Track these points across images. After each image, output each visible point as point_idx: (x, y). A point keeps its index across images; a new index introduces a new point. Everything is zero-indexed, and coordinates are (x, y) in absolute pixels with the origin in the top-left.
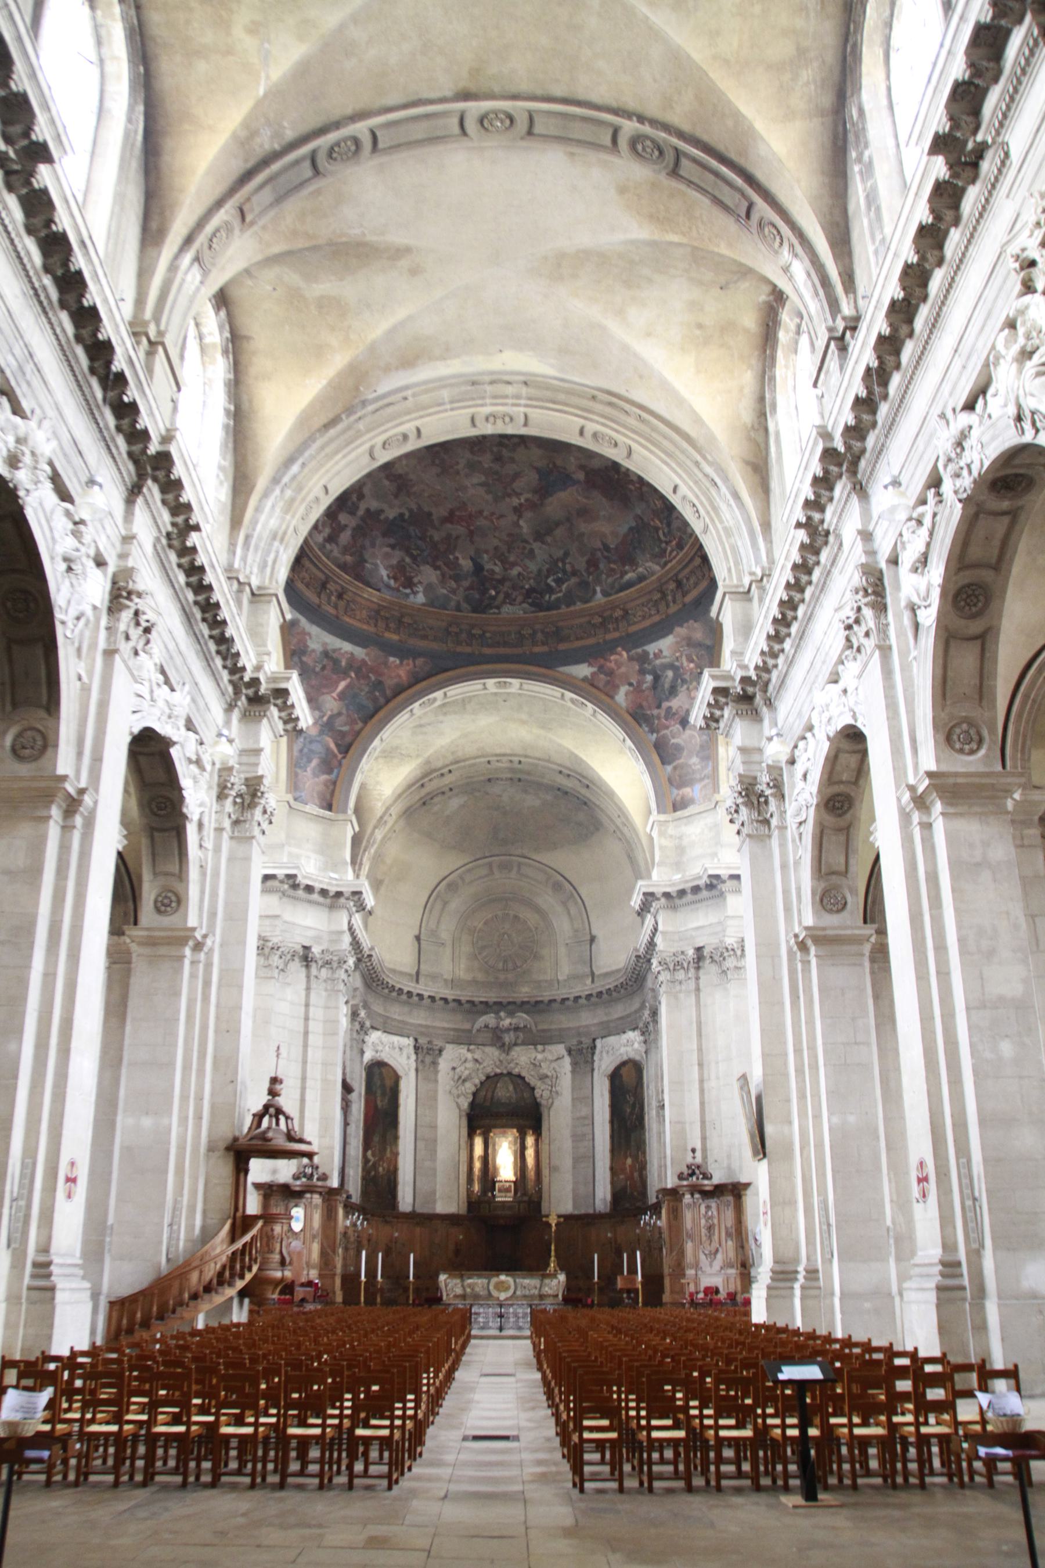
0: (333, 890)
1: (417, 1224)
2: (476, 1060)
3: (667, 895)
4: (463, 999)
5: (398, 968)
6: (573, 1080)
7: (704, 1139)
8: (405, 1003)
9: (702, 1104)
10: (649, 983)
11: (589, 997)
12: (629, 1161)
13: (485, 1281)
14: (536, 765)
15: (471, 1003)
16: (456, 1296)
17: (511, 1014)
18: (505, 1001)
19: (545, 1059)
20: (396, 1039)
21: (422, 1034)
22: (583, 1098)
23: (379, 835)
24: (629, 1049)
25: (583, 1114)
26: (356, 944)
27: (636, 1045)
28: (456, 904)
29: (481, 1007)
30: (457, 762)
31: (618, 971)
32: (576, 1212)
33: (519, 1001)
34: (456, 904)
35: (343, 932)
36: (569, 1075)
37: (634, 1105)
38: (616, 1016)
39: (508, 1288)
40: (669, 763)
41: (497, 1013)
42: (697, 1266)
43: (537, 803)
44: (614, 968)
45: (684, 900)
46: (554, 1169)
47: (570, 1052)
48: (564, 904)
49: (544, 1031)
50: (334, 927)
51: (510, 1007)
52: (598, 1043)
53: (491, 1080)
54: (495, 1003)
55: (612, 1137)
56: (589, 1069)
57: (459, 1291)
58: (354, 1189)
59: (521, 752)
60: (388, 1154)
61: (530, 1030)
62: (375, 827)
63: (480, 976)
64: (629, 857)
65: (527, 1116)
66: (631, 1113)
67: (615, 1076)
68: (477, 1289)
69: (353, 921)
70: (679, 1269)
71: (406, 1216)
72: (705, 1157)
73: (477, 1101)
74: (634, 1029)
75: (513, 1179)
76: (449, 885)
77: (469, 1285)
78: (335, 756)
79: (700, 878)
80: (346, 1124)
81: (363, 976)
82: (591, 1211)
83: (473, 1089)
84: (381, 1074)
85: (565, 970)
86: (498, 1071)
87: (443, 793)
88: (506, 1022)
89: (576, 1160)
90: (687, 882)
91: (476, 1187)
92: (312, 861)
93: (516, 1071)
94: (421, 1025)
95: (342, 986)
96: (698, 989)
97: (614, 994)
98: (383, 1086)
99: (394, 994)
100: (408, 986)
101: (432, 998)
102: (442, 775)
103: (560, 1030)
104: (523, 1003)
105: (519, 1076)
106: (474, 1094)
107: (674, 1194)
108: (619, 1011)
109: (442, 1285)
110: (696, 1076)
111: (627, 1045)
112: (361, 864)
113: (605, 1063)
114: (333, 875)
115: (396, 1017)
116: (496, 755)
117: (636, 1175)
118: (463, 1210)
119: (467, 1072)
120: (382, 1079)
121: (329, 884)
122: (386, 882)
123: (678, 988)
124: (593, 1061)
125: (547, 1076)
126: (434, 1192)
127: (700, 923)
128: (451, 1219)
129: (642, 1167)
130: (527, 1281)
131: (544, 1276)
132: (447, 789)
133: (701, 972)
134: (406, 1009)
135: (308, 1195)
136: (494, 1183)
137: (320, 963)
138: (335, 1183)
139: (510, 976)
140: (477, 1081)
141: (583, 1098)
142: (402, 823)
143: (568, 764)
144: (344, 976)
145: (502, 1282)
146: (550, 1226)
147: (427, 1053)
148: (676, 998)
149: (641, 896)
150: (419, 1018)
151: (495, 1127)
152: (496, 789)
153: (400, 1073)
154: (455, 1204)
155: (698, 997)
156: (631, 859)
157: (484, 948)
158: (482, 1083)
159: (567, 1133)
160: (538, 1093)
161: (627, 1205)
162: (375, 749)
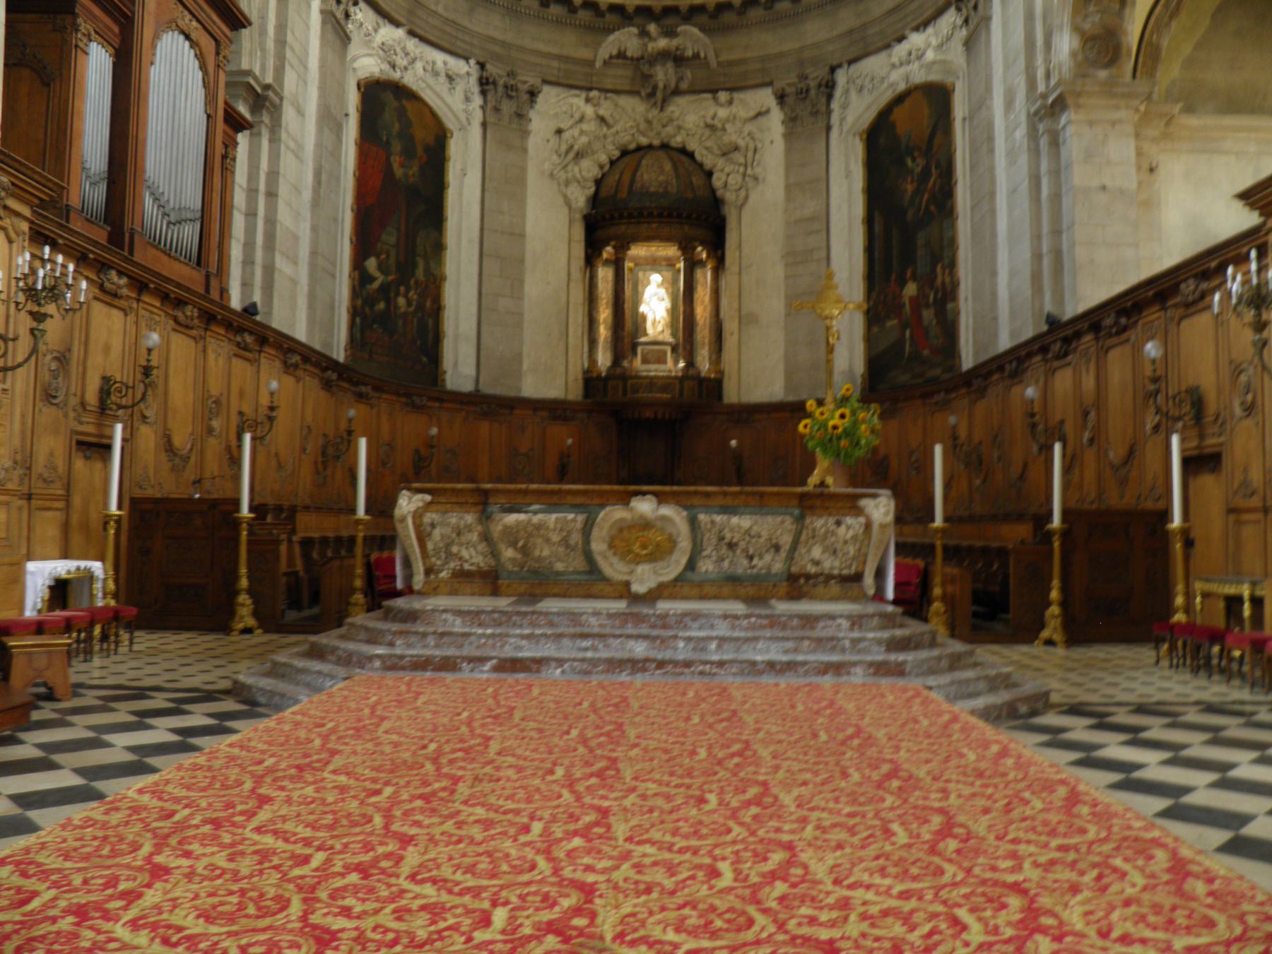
2: (602, 119)
6: (788, 151)
12: (911, 289)
13: (574, 519)
17: (670, 33)
19: (732, 119)
20: (440, 58)
21: (497, 57)
22: (808, 182)
27: (930, 55)
29: (610, 18)
37: (926, 173)
38: (885, 8)
39: (657, 554)
46: (746, 320)
47: (781, 98)
49: (730, 63)
52: (841, 77)
55: (869, 250)
57: (473, 556)
60: (420, 272)
61: (706, 64)
65: (699, 223)
66: (918, 191)
73: (603, 194)
77: (511, 536)
83: (595, 172)
84: (402, 113)
86: (644, 141)
88: (663, 43)
91: (604, 359)
93: (677, 141)
94: (493, 40)
106: (598, 182)
109: (408, 532)
113: (855, 108)
115: (440, 10)
117: (928, 315)
118: (575, 393)
119: (584, 139)
124: (829, 112)
125: (737, 148)
126: (518, 358)
128: (554, 410)
130: (742, 522)
136: (634, 346)
140: (604, 158)
141: (808, 182)
145: (645, 524)
147: (505, 95)
153: (450, 123)
154: (560, 382)
158: (612, 163)
160: (717, 181)
161: (904, 378)
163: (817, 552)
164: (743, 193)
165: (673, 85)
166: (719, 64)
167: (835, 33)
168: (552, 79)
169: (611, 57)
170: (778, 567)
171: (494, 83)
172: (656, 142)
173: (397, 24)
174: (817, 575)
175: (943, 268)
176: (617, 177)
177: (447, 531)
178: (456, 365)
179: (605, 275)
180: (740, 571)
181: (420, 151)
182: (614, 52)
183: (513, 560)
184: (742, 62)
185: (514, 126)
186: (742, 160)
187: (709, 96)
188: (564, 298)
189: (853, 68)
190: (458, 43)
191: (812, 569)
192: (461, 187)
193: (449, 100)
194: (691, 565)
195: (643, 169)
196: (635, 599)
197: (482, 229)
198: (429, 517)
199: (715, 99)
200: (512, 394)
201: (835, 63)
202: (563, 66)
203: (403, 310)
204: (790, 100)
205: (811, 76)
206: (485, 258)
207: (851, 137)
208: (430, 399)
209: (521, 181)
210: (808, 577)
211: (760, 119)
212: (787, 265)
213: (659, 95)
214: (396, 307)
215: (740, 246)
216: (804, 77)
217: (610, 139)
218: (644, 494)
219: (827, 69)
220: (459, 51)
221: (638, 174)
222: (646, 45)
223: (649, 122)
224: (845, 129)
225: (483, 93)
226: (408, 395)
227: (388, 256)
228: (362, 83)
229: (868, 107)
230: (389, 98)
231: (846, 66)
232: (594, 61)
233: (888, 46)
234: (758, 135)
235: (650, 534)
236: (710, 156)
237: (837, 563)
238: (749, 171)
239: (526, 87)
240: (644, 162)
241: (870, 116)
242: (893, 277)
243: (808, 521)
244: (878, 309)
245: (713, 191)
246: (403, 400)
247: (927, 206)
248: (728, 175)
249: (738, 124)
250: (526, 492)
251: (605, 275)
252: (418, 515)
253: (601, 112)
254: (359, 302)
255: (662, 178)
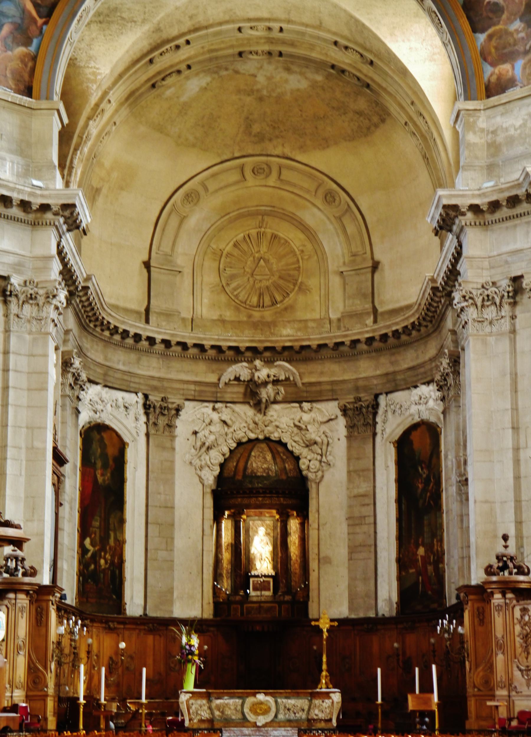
0: (36, 202)
1: (150, 631)
2: (224, 422)
3: (475, 209)
4: (207, 344)
5: (121, 304)
6: (349, 448)
7: (519, 523)
8: (132, 349)
9: (517, 478)
10: (449, 323)
11: (370, 341)
12: (421, 551)
13: (239, 701)
14: (303, 34)
15: (218, 349)
16: (201, 721)
17: (269, 362)
18: (260, 346)
20: (119, 395)
21: (155, 389)
23: (94, 129)
24: (422, 408)
25: (362, 491)
26: (67, 274)
27: (431, 403)
28: (198, 218)
30: (196, 30)
31: (408, 307)
32: (353, 616)
33: (278, 346)
34: (198, 218)
35: (52, 257)
36: (344, 442)
37: (427, 481)
38: (406, 366)
39: (266, 712)
40: (482, 31)
41: (250, 361)
42: (510, 685)
43: (304, 84)
44: (403, 303)
45: (498, 215)
46: (323, 561)
47: (344, 411)
48: (339, 219)
49: (311, 384)
50: (39, 251)
51: (267, 354)
52: (382, 400)
53: (244, 447)
54: (248, 349)
55: (399, 520)
56: (369, 433)
57: (205, 714)
58: (69, 586)
59: (283, 16)
60: (112, 542)
61: (295, 384)
62: (89, 118)
63: (229, 315)
64: (425, 157)
65: (291, 494)
66: (425, 490)
67: (403, 444)
68: (228, 712)
69: (63, 243)
70: (488, 689)
71: (134, 621)
72: (520, 546)
73: (226, 474)
74: (428, 383)
75: (272, 572)
76: (188, 196)
77: (218, 708)
78: (35, 22)
79: (519, 186)
80: (58, 504)
81: (77, 315)
82: (372, 615)
83: (221, 459)
84: (102, 440)
85: (337, 309)
86: (252, 436)
87: (179, 72)
88: (263, 373)
89: (353, 550)
90: (501, 191)
91: (226, 585)
92: (8, 165)
93: (275, 436)
94: (152, 378)
95: (51, 328)
96: (513, 331)
97: (404, 338)
98: (104, 456)
99: (117, 337)
100: (135, 326)
101: (167, 343)
102: (178, 47)
103: (332, 383)
104: (285, 348)
105: (280, 442)
106: (222, 466)
107: (481, 592)
108: (408, 359)
109: (183, 707)
110: (509, 442)
111: (421, 402)
112: (71, 168)
113: (391, 425)
114: (35, 182)
115: (121, 367)
116: (249, 20)
117: (430, 568)
118: (208, 614)
119: (212, 438)
120: (103, 447)
121: (31, 194)
122: (104, 191)
123: (488, 329)
124: (375, 423)
125: (316, 443)
126: (171, 591)
127: (519, 245)
129: (437, 558)
130: (291, 702)
131: (314, 696)
132: (183, 67)
133: (518, 309)
134: (133, 356)
135: (11, 595)
136: (247, 577)
137: (22, 298)
138: (46, 580)
139: (268, 315)
141: (362, 471)
142: (124, 112)
143: (346, 33)
144: (53, 315)
145: (261, 703)
146: (321, 631)
147: (160, 413)
148: (485, 343)
149: (440, 210)
150: (150, 368)
151: (248, 507)
152: (248, 66)
153: (126, 438)
155: (513, 342)
156: (428, 159)
157: (232, 277)
158: (231, 451)
159: (341, 515)
160: (303, 464)
162: (87, 11)
163: (317, 712)
164: (320, 474)
165: (272, 399)
166: (303, 384)
167: (378, 372)
168: (191, 397)
169: (230, 380)
170: (304, 716)
171: (154, 407)
172: (261, 437)
173: (97, 383)
174: (317, 720)
175: (437, 541)
176: (235, 464)
177: (197, 706)
178: (132, 598)
179: (226, 525)
180: (292, 718)
181: (111, 462)
182: (232, 378)
183: (219, 716)
184: (319, 383)
185: (166, 433)
186: (320, 452)
187: (297, 405)
188: (200, 548)
189: (390, 396)
190: (132, 385)
191: (315, 717)
192: (134, 479)
193: (125, 422)
194: (276, 716)
195: (252, 459)
196: (259, 727)
197: (147, 506)
198: (191, 701)
199: (301, 408)
200: (167, 615)
201: (378, 392)
202: (197, 388)
203: (103, 567)
204: (350, 413)
205: (363, 399)
206: (149, 526)
207: (388, 443)
208: (119, 623)
209: (171, 470)
210: (314, 720)
211: (331, 422)
212: (349, 525)
213: (263, 406)
214: (100, 566)
215: (318, 511)
216: (359, 399)
217: (230, 436)
218: (260, 693)
219: (373, 397)
220: (132, 390)
221: (249, 463)
222: (253, 375)
223: (256, 423)
224: (385, 436)
225: (147, 414)
226: (107, 622)
227: (95, 534)
228: (83, 431)
229: (399, 425)
230: (95, 435)
231: (385, 395)
232: (218, 384)
233: (408, 388)
234: (329, 434)
235: (263, 707)
236: (297, 447)
237: (323, 715)
238: (324, 459)
239: (174, 406)
240: (253, 454)
241: (399, 432)
242: (412, 541)
243: (313, 701)
244: (403, 562)
245: (300, 471)
246: (104, 625)
247: (429, 502)
248: (310, 461)
249: (316, 425)
250: (223, 693)
251: (226, 525)
252: (187, 701)
253: (223, 418)
254: (82, 567)
255: (265, 466)
